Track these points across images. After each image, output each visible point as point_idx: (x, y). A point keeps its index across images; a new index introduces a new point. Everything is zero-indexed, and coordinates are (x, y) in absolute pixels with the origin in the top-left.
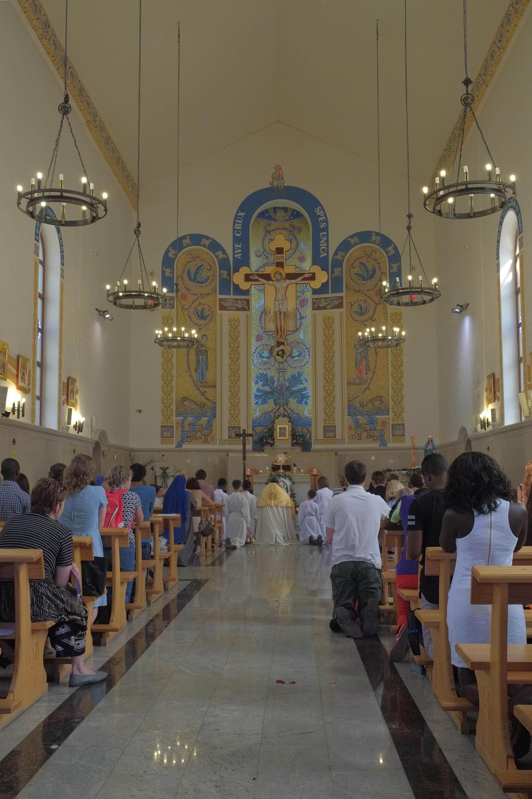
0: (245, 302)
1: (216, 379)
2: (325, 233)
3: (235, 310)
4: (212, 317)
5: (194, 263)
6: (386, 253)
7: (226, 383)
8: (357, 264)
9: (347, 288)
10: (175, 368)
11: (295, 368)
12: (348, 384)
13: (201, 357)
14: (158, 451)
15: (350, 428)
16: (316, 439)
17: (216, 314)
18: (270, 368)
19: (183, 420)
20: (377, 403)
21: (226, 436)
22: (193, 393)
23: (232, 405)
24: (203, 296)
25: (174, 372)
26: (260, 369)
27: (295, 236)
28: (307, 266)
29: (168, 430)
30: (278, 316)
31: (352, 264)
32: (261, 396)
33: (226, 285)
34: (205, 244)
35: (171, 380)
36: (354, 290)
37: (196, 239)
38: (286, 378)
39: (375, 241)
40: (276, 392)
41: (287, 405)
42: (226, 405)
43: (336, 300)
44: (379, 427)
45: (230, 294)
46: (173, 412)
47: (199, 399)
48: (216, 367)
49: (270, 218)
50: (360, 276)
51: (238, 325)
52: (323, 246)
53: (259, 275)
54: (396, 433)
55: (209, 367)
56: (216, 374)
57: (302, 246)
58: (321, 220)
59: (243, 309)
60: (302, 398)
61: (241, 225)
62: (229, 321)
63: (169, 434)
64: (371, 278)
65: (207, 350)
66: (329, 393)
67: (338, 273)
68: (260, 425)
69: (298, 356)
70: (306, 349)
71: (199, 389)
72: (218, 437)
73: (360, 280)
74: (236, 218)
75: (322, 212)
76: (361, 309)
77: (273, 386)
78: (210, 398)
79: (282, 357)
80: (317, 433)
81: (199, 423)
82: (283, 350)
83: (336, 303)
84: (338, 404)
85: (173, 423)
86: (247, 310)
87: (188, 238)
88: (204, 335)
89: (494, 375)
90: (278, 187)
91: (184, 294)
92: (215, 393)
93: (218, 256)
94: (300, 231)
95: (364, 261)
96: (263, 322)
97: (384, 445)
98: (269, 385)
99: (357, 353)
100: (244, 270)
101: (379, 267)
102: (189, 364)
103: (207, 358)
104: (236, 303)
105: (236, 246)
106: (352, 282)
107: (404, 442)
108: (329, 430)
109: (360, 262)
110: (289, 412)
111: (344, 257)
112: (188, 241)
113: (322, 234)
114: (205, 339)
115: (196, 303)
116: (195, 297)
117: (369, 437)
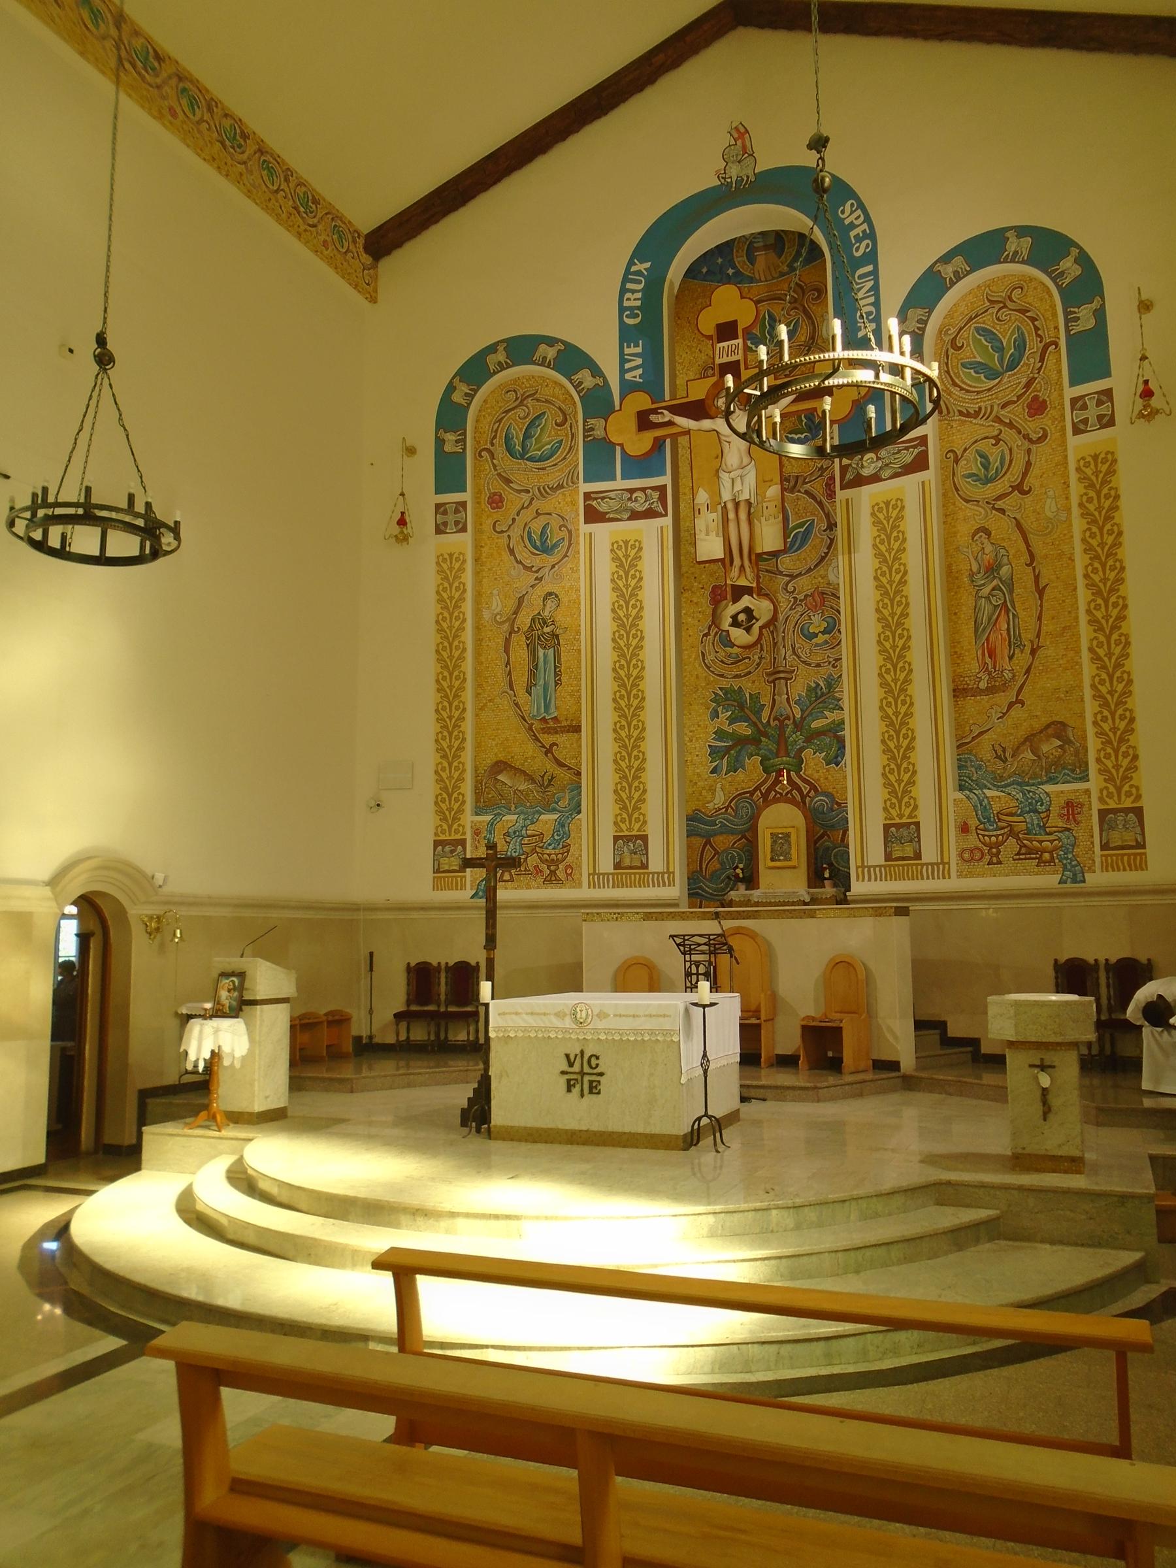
0: (656, 495)
2: (870, 268)
3: (629, 519)
4: (570, 545)
5: (520, 412)
6: (1054, 280)
7: (606, 717)
8: (969, 333)
11: (818, 665)
12: (959, 692)
13: (541, 652)
14: (422, 909)
15: (964, 829)
16: (863, 867)
18: (750, 673)
19: (491, 824)
20: (1050, 747)
21: (606, 864)
22: (526, 752)
24: (545, 492)
25: (468, 696)
26: (722, 676)
27: (805, 311)
29: (452, 852)
30: (731, 515)
32: (728, 749)
37: (521, 348)
39: (1016, 253)
40: (766, 735)
41: (798, 770)
43: (907, 449)
44: (1055, 821)
45: (614, 478)
46: (464, 802)
47: (539, 764)
50: (979, 367)
54: (1116, 838)
59: (650, 514)
61: (639, 295)
64: (1012, 366)
68: (725, 830)
69: (823, 633)
71: (538, 740)
72: (585, 870)
73: (978, 380)
74: (625, 280)
75: (859, 212)
76: (986, 467)
80: (866, 843)
81: (532, 829)
82: (748, 611)
84: (923, 757)
85: (464, 833)
86: (662, 516)
87: (501, 348)
88: (550, 594)
90: (739, 180)
91: (495, 494)
93: (581, 383)
94: (819, 297)
95: (988, 321)
97: (1074, 881)
98: (747, 719)
99: (977, 597)
102: (510, 674)
103: (557, 654)
104: (630, 499)
105: (627, 351)
107: (1142, 866)
108: (901, 835)
109: (977, 329)
110: (805, 788)
117: (1026, 853)
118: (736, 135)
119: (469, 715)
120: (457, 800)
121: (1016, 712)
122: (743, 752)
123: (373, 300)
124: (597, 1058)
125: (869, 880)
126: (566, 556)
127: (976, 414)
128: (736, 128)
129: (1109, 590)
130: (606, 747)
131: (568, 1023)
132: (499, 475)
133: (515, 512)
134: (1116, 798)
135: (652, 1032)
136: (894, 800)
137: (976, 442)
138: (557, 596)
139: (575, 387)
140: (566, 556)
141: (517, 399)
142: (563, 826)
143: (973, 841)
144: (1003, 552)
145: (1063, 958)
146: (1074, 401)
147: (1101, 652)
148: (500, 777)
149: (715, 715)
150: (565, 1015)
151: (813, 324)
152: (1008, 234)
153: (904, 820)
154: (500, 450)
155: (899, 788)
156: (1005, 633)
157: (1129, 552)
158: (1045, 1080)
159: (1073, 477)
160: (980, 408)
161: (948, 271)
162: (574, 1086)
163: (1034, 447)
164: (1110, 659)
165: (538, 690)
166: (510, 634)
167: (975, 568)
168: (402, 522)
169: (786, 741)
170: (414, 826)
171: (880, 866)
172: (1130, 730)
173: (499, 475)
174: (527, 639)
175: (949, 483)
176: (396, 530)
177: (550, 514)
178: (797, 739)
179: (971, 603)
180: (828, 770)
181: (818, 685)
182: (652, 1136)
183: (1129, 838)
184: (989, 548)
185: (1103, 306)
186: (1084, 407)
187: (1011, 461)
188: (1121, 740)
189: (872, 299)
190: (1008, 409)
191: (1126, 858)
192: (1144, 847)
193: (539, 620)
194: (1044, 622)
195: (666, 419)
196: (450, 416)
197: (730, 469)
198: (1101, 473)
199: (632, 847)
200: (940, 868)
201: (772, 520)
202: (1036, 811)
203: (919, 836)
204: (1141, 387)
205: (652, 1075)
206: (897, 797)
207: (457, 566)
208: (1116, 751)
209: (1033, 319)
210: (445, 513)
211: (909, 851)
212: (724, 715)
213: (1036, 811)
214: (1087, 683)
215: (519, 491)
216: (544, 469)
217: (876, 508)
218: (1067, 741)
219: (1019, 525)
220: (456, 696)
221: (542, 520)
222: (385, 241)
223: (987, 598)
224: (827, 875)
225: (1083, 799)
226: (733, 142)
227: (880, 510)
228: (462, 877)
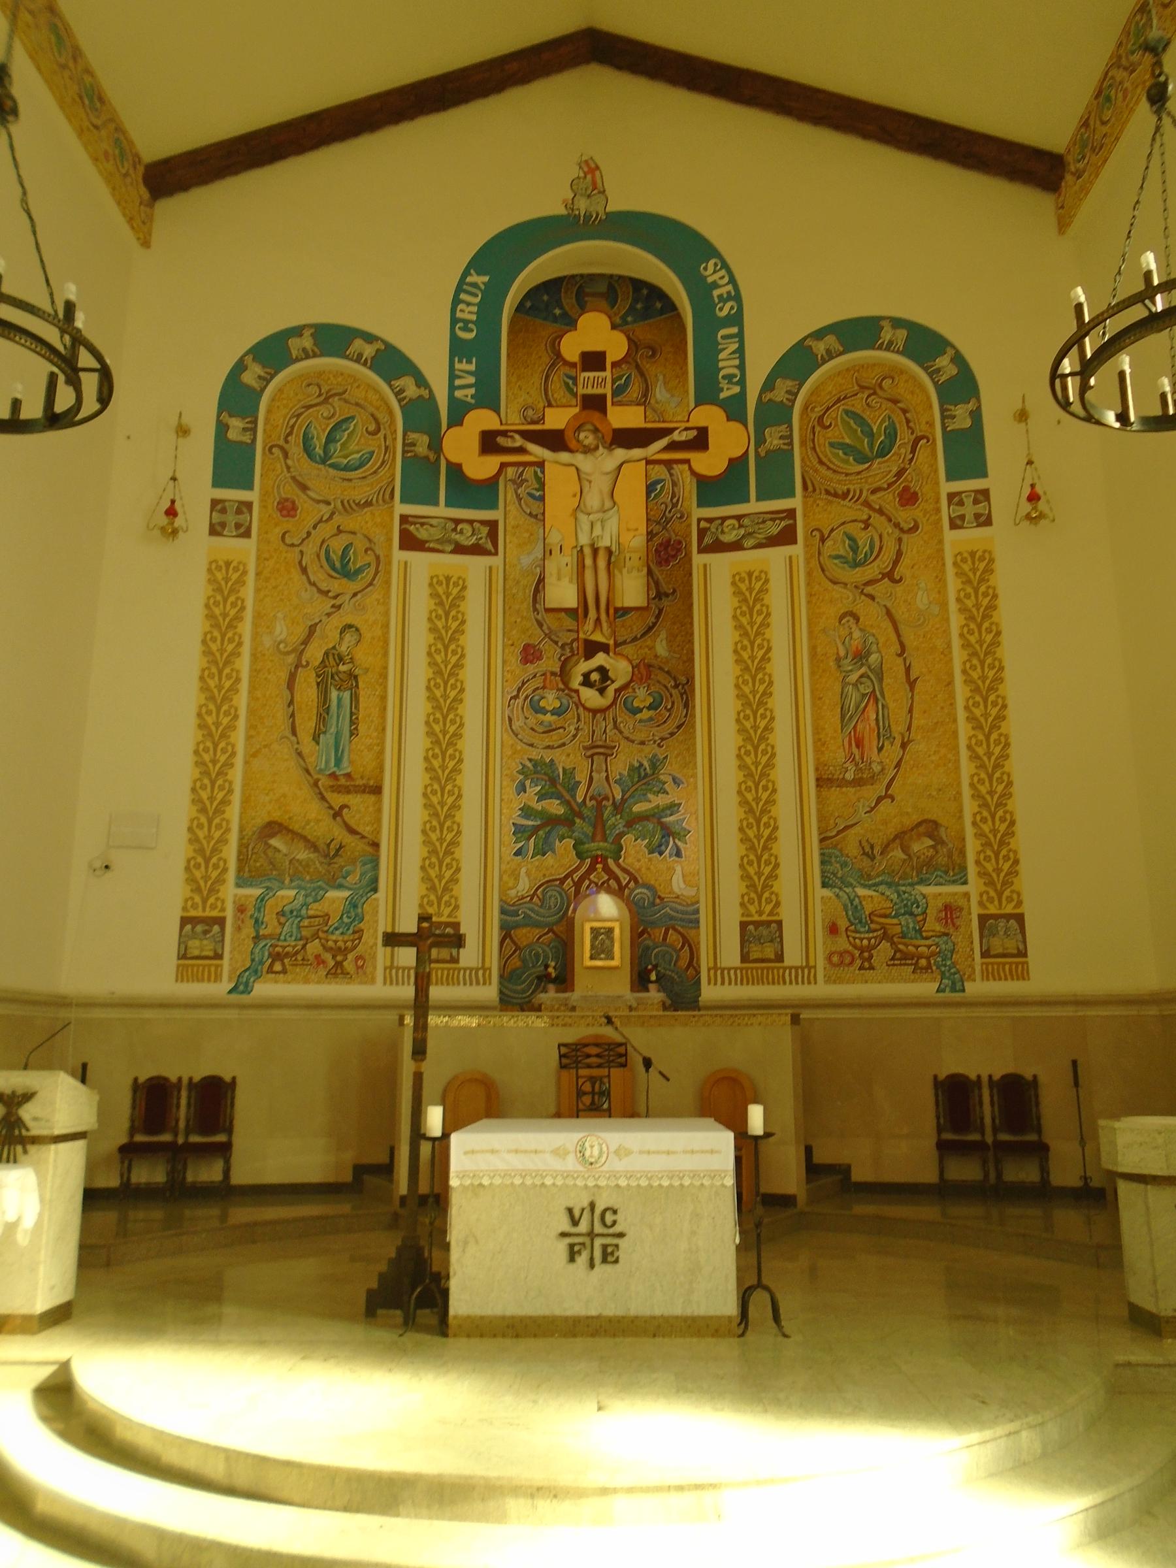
0: (485, 530)
1: (381, 768)
2: (735, 330)
3: (454, 552)
5: (324, 411)
6: (931, 375)
7: (415, 778)
9: (805, 487)
10: (241, 723)
11: (643, 743)
12: (821, 782)
13: (334, 694)
15: (833, 929)
16: (715, 968)
17: (389, 557)
18: (564, 745)
19: (262, 899)
20: (921, 846)
22: (307, 812)
23: (434, 852)
24: (349, 507)
25: (239, 737)
26: (532, 745)
27: (638, 367)
29: (205, 932)
30: (588, 561)
32: (536, 829)
34: (360, 355)
35: (229, 764)
36: (828, 492)
37: (333, 339)
38: (614, 775)
39: (891, 343)
40: (580, 815)
41: (617, 858)
42: (413, 852)
43: (773, 520)
44: (933, 925)
45: (436, 504)
46: (225, 870)
47: (324, 828)
48: (384, 729)
50: (847, 449)
51: (460, 597)
52: (727, 364)
53: (525, 435)
55: (362, 728)
56: (382, 752)
57: (660, 393)
58: (720, 296)
59: (476, 550)
60: (664, 834)
61: (475, 309)
62: (431, 585)
63: (208, 948)
64: (883, 452)
65: (357, 672)
67: (775, 442)
69: (649, 708)
70: (676, 686)
71: (323, 798)
73: (847, 462)
74: (459, 289)
75: (723, 272)
76: (855, 548)
77: (574, 797)
78: (360, 829)
79: (602, 691)
82: (602, 670)
83: (774, 529)
84: (787, 848)
85: (223, 910)
87: (307, 333)
88: (350, 626)
90: (588, 216)
91: (287, 500)
92: (379, 810)
94: (653, 355)
95: (857, 404)
97: (953, 990)
98: (559, 796)
99: (844, 684)
101: (908, 421)
102: (293, 715)
103: (355, 698)
104: (454, 530)
105: (457, 366)
106: (823, 470)
107: (1024, 975)
108: (761, 934)
109: (847, 412)
110: (625, 878)
111: (796, 394)
112: (307, 342)
113: (722, 332)
114: (349, 638)
115: (326, 530)
116: (325, 510)
117: (901, 958)
118: (586, 169)
119: (239, 761)
120: (216, 866)
121: (885, 805)
122: (554, 834)
123: (146, 244)
124: (615, 1212)
125: (723, 983)
126: (371, 584)
127: (845, 495)
128: (586, 162)
129: (988, 687)
130: (414, 815)
131: (571, 1163)
132: (293, 478)
133: (312, 523)
134: (996, 902)
135: (695, 1174)
136: (753, 895)
137: (844, 523)
138: (357, 630)
139: (397, 394)
140: (371, 584)
141: (320, 395)
142: (355, 906)
143: (842, 943)
144: (871, 639)
145: (942, 1076)
146: (951, 496)
147: (981, 751)
148: (274, 842)
149: (522, 788)
150: (567, 1153)
151: (646, 380)
152: (883, 323)
153: (764, 918)
154: (296, 450)
155: (759, 881)
156: (873, 724)
157: (1008, 651)
159: (950, 571)
160: (848, 491)
161: (820, 347)
162: (579, 1252)
163: (905, 537)
164: (989, 758)
165: (327, 739)
166: (297, 667)
167: (842, 653)
168: (171, 512)
169: (604, 826)
170: (157, 893)
171: (736, 969)
173: (293, 478)
174: (318, 676)
175: (814, 563)
176: (164, 520)
177: (354, 533)
178: (616, 822)
179: (838, 688)
180: (650, 860)
181: (641, 765)
182: (694, 1319)
183: (1011, 945)
184: (857, 634)
185: (979, 408)
186: (961, 503)
187: (881, 548)
188: (1002, 843)
189: (737, 362)
190: (879, 495)
191: (1007, 967)
192: (1025, 955)
193: (333, 656)
194: (915, 715)
195: (517, 444)
196: (237, 398)
197: (589, 510)
198: (979, 570)
200: (805, 972)
201: (635, 573)
202: (912, 914)
203: (781, 937)
204: (1027, 491)
205: (693, 1233)
206: (756, 892)
207: (235, 576)
208: (997, 854)
209: (904, 411)
210: (223, 511)
211: (769, 952)
212: (533, 790)
213: (912, 914)
215: (318, 502)
216: (350, 480)
217: (737, 578)
218: (939, 842)
219: (889, 613)
220: (223, 736)
221: (343, 540)
222: (170, 177)
223: (855, 685)
224: (653, 977)
225: (962, 902)
226: (582, 175)
227: (742, 580)
228: (217, 966)
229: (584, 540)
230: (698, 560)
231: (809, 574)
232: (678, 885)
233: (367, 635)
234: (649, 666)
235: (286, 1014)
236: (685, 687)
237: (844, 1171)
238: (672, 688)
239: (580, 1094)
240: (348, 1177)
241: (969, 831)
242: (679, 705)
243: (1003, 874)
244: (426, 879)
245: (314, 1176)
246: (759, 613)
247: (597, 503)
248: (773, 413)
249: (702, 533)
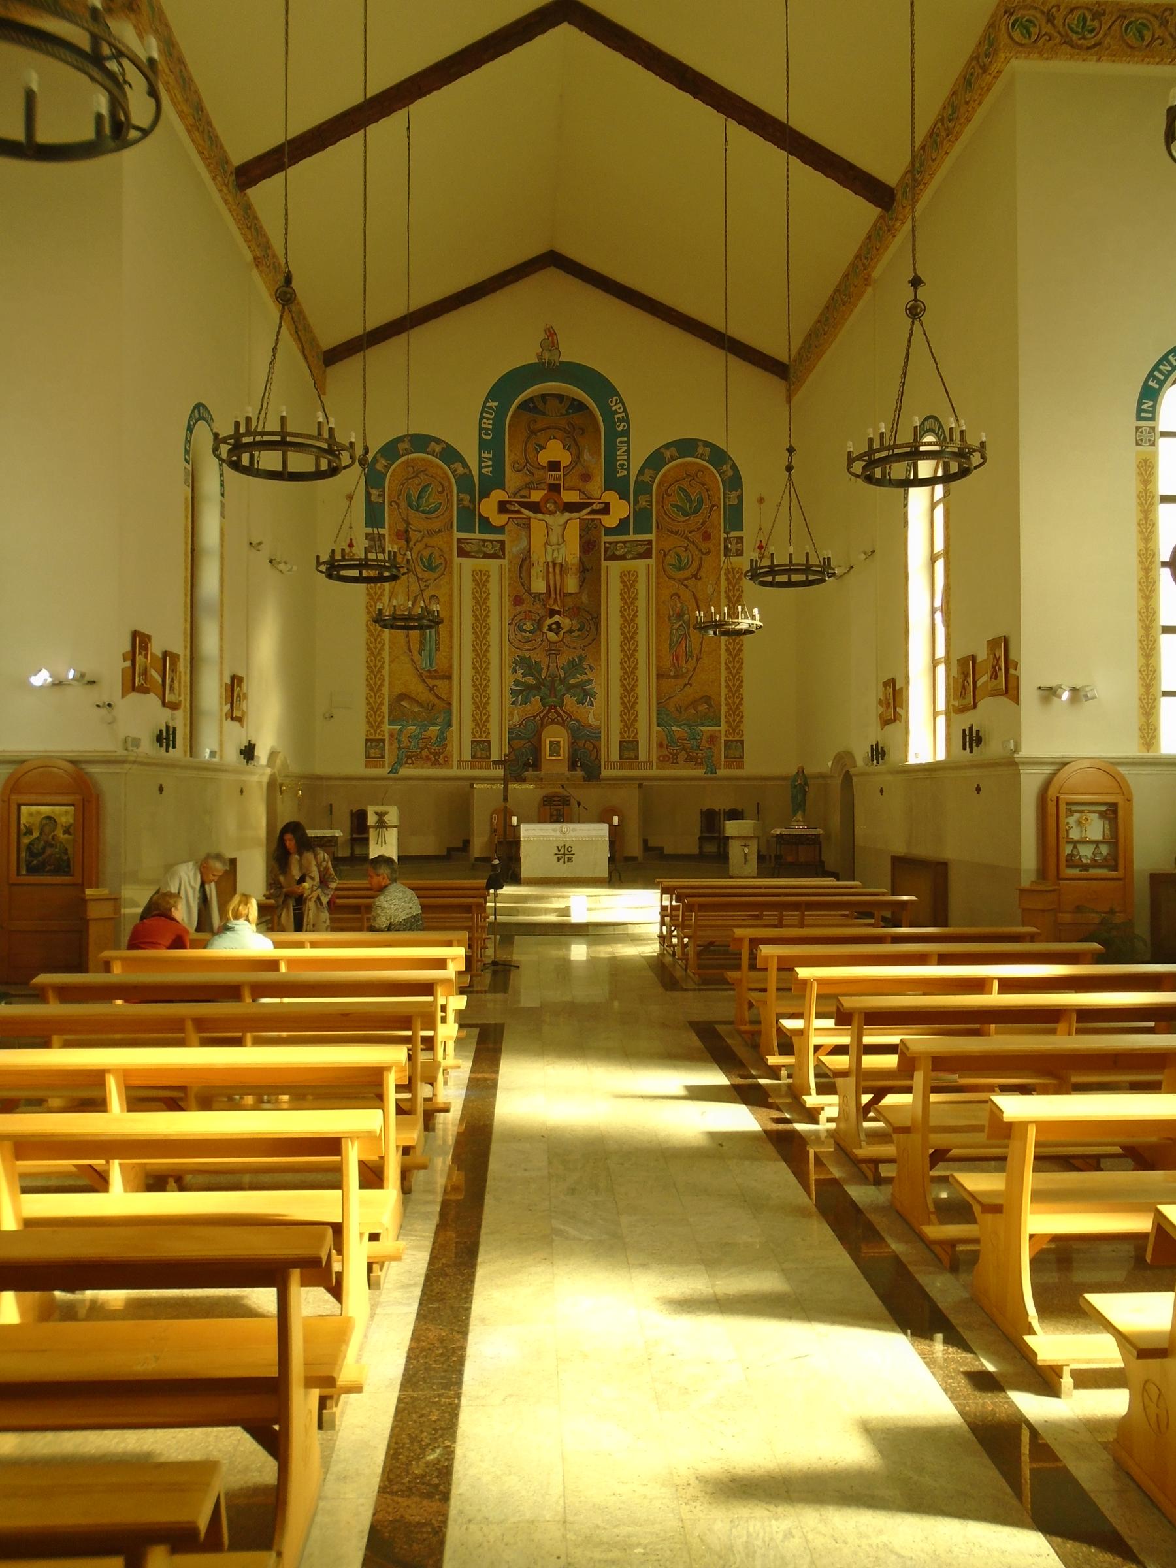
0: (498, 545)
1: (451, 667)
7: (468, 672)
8: (675, 488)
9: (657, 527)
10: (387, 647)
15: (661, 745)
17: (452, 563)
20: (703, 707)
21: (467, 756)
22: (417, 688)
23: (477, 708)
24: (431, 533)
25: (386, 654)
28: (596, 487)
31: (667, 491)
32: (522, 691)
33: (469, 517)
35: (382, 667)
37: (420, 442)
44: (704, 744)
47: (425, 696)
49: (535, 410)
50: (679, 508)
51: (487, 581)
52: (621, 459)
53: (520, 504)
54: (731, 753)
55: (441, 647)
57: (586, 456)
59: (494, 556)
60: (585, 695)
64: (696, 511)
66: (629, 690)
68: (518, 737)
74: (483, 411)
76: (680, 561)
79: (557, 634)
80: (611, 750)
81: (425, 734)
82: (557, 623)
83: (641, 549)
84: (642, 708)
86: (500, 558)
88: (433, 596)
89: (893, 681)
95: (684, 485)
96: (524, 575)
100: (498, 495)
103: (437, 633)
107: (742, 767)
108: (629, 747)
112: (406, 445)
116: (419, 535)
117: (689, 759)
119: (386, 665)
121: (688, 689)
127: (676, 533)
130: (468, 691)
131: (558, 833)
154: (403, 504)
155: (629, 724)
158: (746, 851)
159: (723, 577)
172: (740, 704)
178: (561, 688)
184: (679, 605)
199: (481, 746)
200: (648, 764)
211: (632, 755)
214: (723, 679)
218: (711, 706)
219: (694, 595)
222: (334, 356)
229: (549, 559)
230: (604, 563)
231: (657, 572)
232: (591, 720)
233: (442, 600)
234: (578, 608)
235: (415, 782)
236: (596, 620)
237: (662, 849)
238: (589, 619)
239: (552, 815)
240: (445, 853)
241: (723, 702)
242: (593, 629)
243: (736, 724)
244: (475, 720)
245: (430, 851)
246: (631, 588)
247: (555, 540)
248: (643, 488)
249: (606, 549)
